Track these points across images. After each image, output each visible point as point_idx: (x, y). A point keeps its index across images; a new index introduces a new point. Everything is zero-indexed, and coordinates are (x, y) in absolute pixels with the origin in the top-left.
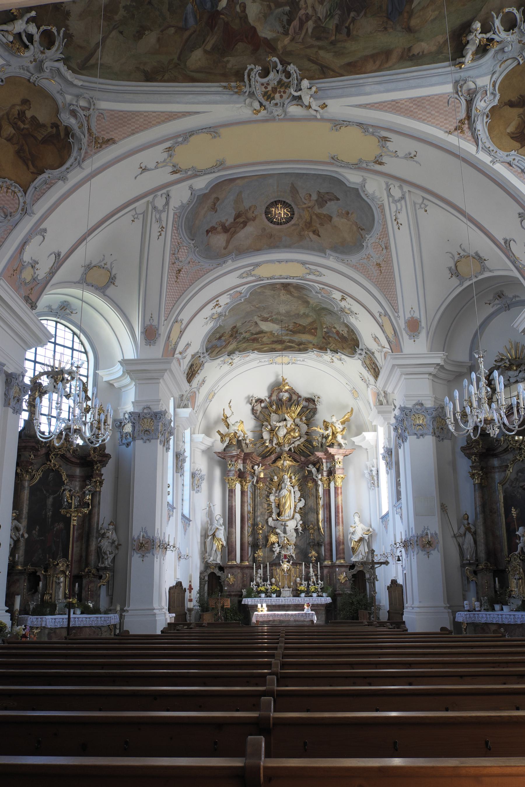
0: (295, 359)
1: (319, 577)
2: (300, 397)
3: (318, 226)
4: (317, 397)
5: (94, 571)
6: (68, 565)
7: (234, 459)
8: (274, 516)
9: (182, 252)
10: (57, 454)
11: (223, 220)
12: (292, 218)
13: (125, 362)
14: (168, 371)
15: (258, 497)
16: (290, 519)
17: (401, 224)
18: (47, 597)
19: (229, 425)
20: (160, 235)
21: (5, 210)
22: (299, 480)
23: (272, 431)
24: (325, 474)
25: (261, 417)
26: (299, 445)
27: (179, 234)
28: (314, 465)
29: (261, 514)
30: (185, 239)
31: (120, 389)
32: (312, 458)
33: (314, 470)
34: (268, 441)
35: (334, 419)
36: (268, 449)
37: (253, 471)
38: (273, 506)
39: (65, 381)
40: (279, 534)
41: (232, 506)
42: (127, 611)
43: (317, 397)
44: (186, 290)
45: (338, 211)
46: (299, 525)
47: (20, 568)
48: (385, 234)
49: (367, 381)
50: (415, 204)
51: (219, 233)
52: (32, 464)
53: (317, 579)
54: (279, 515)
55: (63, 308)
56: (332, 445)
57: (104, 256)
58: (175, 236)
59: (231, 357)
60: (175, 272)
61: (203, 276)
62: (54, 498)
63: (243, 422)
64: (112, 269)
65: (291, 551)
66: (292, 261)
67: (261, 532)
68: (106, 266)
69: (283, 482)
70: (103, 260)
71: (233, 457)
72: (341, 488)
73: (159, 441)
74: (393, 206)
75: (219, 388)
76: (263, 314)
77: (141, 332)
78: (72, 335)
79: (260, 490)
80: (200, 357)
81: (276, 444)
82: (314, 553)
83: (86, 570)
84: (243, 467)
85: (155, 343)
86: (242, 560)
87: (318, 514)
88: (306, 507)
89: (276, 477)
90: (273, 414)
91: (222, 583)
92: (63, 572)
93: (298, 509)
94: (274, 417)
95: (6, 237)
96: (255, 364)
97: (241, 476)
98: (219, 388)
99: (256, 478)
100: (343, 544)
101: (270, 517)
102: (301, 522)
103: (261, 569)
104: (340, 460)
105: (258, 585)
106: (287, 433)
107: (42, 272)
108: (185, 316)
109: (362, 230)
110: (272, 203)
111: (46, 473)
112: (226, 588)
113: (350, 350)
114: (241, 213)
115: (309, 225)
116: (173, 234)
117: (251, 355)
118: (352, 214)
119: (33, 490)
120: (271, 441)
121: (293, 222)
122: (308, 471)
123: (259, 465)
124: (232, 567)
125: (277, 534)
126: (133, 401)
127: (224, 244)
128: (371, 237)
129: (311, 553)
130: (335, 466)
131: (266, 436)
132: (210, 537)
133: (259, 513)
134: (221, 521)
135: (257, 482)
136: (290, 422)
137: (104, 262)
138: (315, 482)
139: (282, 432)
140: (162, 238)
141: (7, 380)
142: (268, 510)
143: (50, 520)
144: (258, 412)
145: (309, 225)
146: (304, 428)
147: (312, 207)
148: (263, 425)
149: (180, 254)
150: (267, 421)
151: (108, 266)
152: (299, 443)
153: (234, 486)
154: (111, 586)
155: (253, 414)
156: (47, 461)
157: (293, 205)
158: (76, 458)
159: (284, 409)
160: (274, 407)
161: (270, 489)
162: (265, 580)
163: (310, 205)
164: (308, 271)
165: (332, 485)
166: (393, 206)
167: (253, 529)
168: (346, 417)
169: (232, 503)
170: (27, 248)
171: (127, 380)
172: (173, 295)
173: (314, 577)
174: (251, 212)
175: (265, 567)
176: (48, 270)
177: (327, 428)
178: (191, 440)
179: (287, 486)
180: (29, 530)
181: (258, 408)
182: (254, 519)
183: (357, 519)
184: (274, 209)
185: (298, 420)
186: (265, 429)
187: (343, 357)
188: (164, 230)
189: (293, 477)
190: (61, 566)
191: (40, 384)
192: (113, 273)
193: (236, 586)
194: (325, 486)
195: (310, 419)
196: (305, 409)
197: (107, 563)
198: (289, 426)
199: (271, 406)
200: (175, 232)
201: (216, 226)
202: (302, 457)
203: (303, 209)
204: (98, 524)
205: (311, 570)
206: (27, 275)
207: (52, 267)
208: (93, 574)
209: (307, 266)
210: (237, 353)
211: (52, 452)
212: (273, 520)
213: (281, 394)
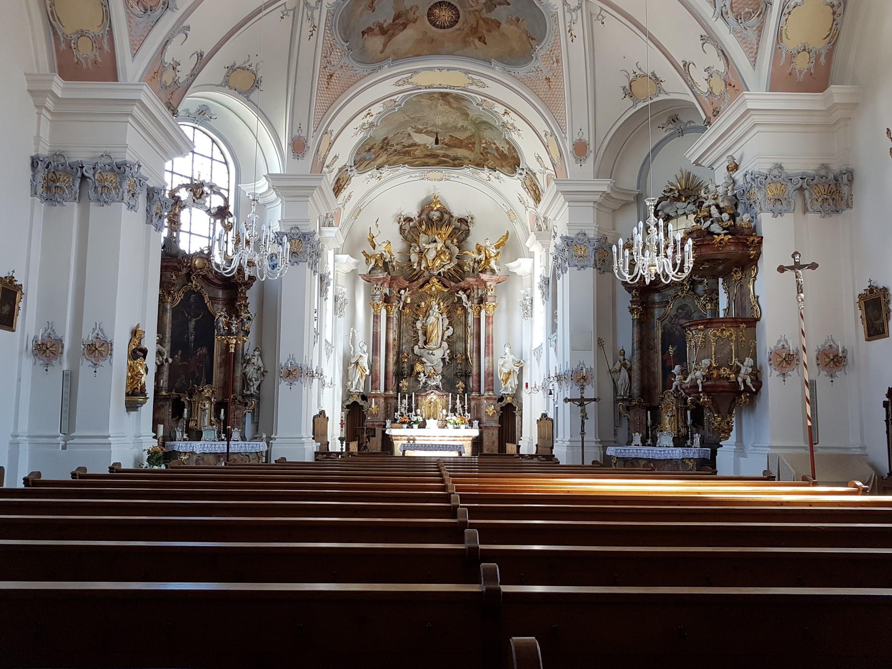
0: (449, 175)
1: (466, 408)
2: (452, 217)
3: (485, 32)
4: (470, 217)
5: (239, 398)
6: (213, 392)
8: (421, 344)
9: (334, 55)
10: (199, 275)
11: (381, 21)
12: (457, 22)
13: (270, 177)
14: (317, 189)
17: (575, 37)
18: (192, 424)
19: (375, 245)
20: (312, 35)
21: (144, 3)
22: (448, 306)
24: (476, 301)
25: (409, 237)
27: (332, 35)
28: (465, 291)
29: (407, 341)
30: (339, 39)
31: (264, 205)
32: (462, 284)
33: (464, 297)
35: (488, 243)
37: (399, 296)
38: (420, 332)
39: (205, 195)
41: (377, 333)
42: (275, 439)
43: (470, 217)
44: (338, 97)
45: (507, 18)
46: (446, 354)
47: (164, 393)
48: (557, 45)
49: (526, 203)
50: (591, 15)
51: (376, 35)
52: (174, 285)
53: (464, 410)
54: (425, 343)
55: (201, 113)
56: (484, 271)
57: (249, 56)
58: (328, 37)
59: (380, 171)
60: (326, 77)
61: (356, 82)
62: (195, 321)
63: (390, 242)
64: (257, 71)
65: (437, 381)
66: (454, 69)
67: (406, 360)
68: (251, 68)
69: (431, 309)
70: (249, 60)
71: (379, 280)
72: (492, 317)
73: (307, 263)
74: (568, 15)
75: (365, 204)
76: (417, 126)
77: (288, 144)
78: (211, 143)
80: (347, 170)
81: (424, 268)
83: (232, 396)
85: (303, 156)
86: (386, 389)
87: (466, 343)
88: (455, 335)
89: (423, 304)
90: (422, 235)
92: (209, 399)
93: (445, 337)
94: (423, 238)
95: (146, 34)
96: (405, 179)
97: (387, 300)
98: (365, 204)
99: (402, 303)
100: (493, 375)
102: (448, 351)
104: (492, 287)
105: (402, 415)
107: (183, 74)
108: (335, 127)
109: (532, 39)
110: (436, 3)
111: (188, 294)
112: (369, 418)
113: (509, 168)
114: (401, 13)
115: (474, 30)
116: (326, 35)
117: (401, 169)
118: (522, 21)
119: (176, 312)
120: (419, 264)
121: (457, 26)
122: (458, 297)
123: (405, 289)
124: (375, 397)
125: (423, 363)
126: (280, 219)
127: (381, 48)
128: (541, 48)
129: (458, 383)
130: (487, 293)
131: (414, 258)
132: (353, 365)
134: (365, 348)
135: (403, 308)
136: (440, 245)
137: (249, 63)
139: (431, 255)
140: (313, 38)
141: (148, 194)
142: (414, 337)
143: (192, 344)
144: (406, 232)
145: (474, 30)
146: (456, 251)
147: (480, 11)
148: (411, 246)
149: (332, 58)
150: (415, 241)
151: (253, 68)
152: (450, 267)
153: (379, 311)
154: (255, 414)
155: (401, 234)
156: (188, 282)
157: (458, 7)
158: (219, 279)
159: (434, 229)
160: (424, 227)
161: (417, 315)
162: (410, 410)
163: (477, 8)
164: (471, 81)
166: (568, 15)
167: (398, 357)
169: (377, 329)
170: (169, 47)
171: (274, 196)
172: (323, 103)
173: (461, 409)
174: (412, 12)
176: (189, 72)
177: (479, 252)
178: (335, 261)
179: (435, 313)
180: (172, 354)
181: (407, 227)
182: (399, 347)
183: (507, 350)
184: (437, 11)
185: (449, 242)
186: (413, 250)
187: (501, 175)
188: (316, 29)
190: (207, 393)
191: (179, 198)
192: (259, 75)
193: (379, 416)
195: (462, 241)
196: (457, 231)
197: (253, 390)
198: (439, 248)
199: (421, 226)
200: (328, 32)
201: (374, 27)
202: (452, 282)
203: (470, 13)
204: (243, 349)
205: (458, 401)
206: (168, 78)
207: (193, 69)
208: (239, 402)
209: (470, 75)
210: (387, 166)
211: (193, 273)
212: (420, 348)
213: (433, 213)
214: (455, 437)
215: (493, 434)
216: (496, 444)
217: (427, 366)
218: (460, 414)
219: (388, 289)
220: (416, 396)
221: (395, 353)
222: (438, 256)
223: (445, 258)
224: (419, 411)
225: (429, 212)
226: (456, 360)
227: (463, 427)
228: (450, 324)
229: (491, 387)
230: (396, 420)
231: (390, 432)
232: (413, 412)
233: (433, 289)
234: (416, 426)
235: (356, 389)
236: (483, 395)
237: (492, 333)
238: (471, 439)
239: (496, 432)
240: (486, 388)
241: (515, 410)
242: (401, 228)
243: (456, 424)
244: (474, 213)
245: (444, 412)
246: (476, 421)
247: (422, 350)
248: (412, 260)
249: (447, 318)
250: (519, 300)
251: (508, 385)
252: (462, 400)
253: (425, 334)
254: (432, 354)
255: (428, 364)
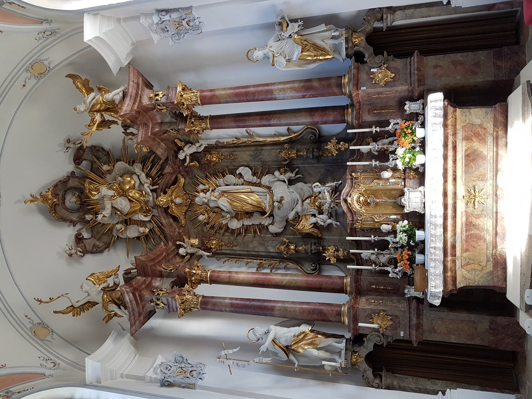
1: (378, 129)
2: (73, 173)
7: (147, 295)
8: (266, 221)
15: (235, 248)
16: (272, 194)
19: (88, 302)
22: (207, 177)
23: (127, 222)
25: (105, 239)
26: (148, 176)
28: (180, 149)
33: (189, 150)
34: (142, 229)
36: (156, 229)
37: (188, 256)
38: (247, 222)
40: (297, 213)
41: (232, 305)
46: (282, 177)
54: (263, 213)
67: (292, 247)
69: (207, 204)
72: (202, 91)
75: (31, 315)
79: (222, 245)
81: (146, 216)
82: (330, 146)
84: (169, 275)
86: (341, 290)
88: (252, 164)
89: (201, 217)
91: (390, 339)
93: (255, 179)
99: (201, 252)
101: (268, 229)
102: (277, 173)
103: (360, 254)
104: (152, 95)
105: (394, 262)
106: (126, 197)
112: (402, 334)
120: (142, 224)
122: (191, 161)
123: (180, 246)
124: (355, 319)
125: (298, 218)
130: (164, 105)
131: (133, 232)
132: (292, 357)
133: (261, 249)
135: (208, 250)
136: (105, 191)
138: (209, 149)
142: (255, 232)
144: (98, 243)
146: (121, 165)
148: (118, 237)
150: (111, 230)
155: (101, 252)
160: (88, 217)
161: (220, 228)
162: (383, 246)
165: (204, 111)
167: (290, 259)
168: (80, 86)
169: (226, 305)
173: (380, 143)
175: (358, 245)
179: (213, 198)
185: (109, 177)
189: (201, 187)
193: (397, 313)
194: (203, 125)
212: (272, 223)
214: (446, 145)
215: (436, 67)
216: (459, 56)
217: (303, 210)
218: (391, 143)
219: (165, 279)
220: (354, 232)
221: (282, 265)
222: (123, 193)
223: (131, 181)
224: (385, 228)
225: (67, 209)
226: (292, 159)
227: (420, 133)
228: (233, 172)
229: (333, 81)
230: (405, 274)
231: (434, 296)
232: (388, 238)
233: (178, 201)
234: (419, 234)
235: (339, 353)
236: (350, 96)
237: (230, 89)
238: (450, 109)
239: (431, 60)
240: (336, 90)
241: (382, 28)
242: (92, 253)
243: (414, 148)
244: (62, 139)
245: (387, 174)
246: (406, 107)
247: (277, 218)
248: (137, 235)
249: (224, 176)
250: (171, 43)
251: (328, 44)
252: (362, 139)
253: (249, 214)
254: (280, 202)
255: (299, 208)
